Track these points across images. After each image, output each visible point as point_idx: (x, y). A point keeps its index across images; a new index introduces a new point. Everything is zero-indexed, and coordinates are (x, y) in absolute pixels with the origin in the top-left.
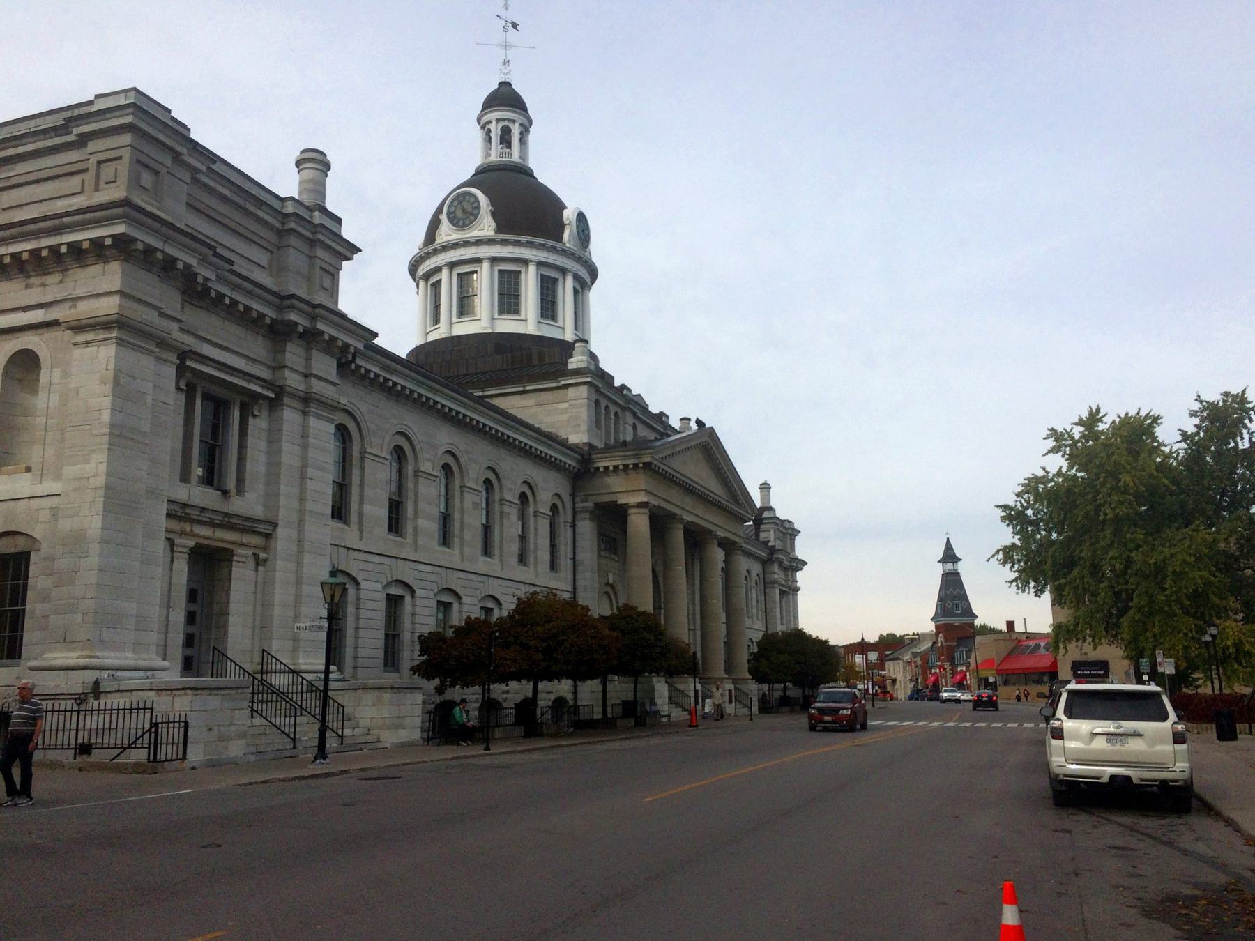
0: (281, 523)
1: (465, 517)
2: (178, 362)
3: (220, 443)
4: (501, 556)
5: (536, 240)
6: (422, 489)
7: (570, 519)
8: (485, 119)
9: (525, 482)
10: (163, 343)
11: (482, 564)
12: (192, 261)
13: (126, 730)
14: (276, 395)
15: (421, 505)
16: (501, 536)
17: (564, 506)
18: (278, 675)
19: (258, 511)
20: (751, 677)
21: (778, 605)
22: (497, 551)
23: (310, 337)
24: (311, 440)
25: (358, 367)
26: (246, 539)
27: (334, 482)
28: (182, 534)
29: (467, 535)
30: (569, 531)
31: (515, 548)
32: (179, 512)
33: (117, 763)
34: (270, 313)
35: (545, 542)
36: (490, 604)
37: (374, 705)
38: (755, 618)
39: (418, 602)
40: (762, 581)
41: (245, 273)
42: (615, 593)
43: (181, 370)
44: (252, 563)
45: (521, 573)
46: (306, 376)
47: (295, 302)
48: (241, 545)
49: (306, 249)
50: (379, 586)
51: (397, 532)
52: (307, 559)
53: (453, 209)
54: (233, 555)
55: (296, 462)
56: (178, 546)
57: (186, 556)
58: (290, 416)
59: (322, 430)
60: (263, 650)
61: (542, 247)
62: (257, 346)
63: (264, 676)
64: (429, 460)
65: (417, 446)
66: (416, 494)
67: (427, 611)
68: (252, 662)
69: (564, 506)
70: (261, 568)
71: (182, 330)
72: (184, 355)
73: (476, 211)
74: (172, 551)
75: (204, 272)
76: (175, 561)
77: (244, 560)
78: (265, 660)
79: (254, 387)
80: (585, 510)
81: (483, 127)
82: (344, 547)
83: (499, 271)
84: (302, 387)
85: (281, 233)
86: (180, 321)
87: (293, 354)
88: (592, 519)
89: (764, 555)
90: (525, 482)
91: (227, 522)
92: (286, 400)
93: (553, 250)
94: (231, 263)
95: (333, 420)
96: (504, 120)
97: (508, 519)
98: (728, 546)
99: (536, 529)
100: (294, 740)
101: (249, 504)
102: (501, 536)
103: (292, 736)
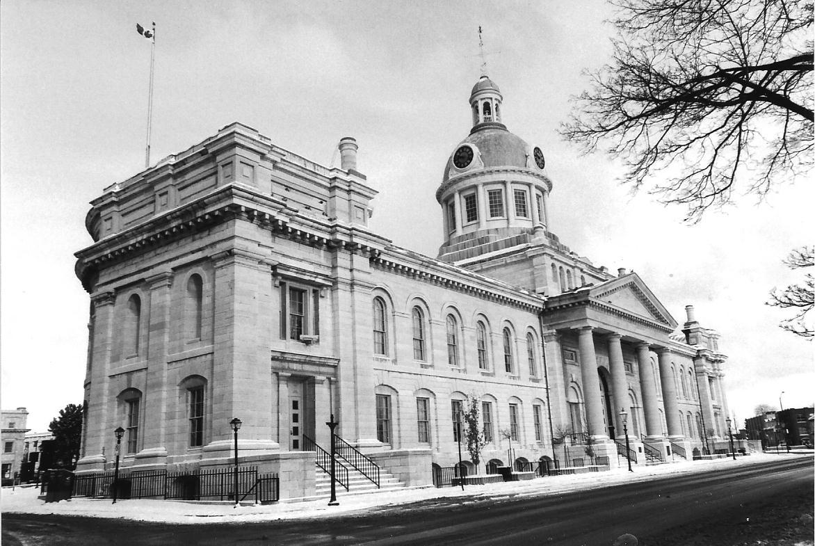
12: (274, 213)
15: (434, 341)
16: (493, 355)
19: (328, 353)
23: (351, 248)
26: (323, 369)
28: (283, 369)
34: (326, 237)
35: (524, 356)
43: (275, 275)
44: (327, 382)
48: (320, 373)
50: (411, 393)
58: (343, 294)
59: (364, 300)
62: (321, 256)
74: (278, 380)
75: (281, 218)
76: (280, 385)
79: (319, 280)
85: (332, 189)
87: (343, 258)
88: (557, 341)
91: (308, 361)
92: (340, 286)
98: (659, 350)
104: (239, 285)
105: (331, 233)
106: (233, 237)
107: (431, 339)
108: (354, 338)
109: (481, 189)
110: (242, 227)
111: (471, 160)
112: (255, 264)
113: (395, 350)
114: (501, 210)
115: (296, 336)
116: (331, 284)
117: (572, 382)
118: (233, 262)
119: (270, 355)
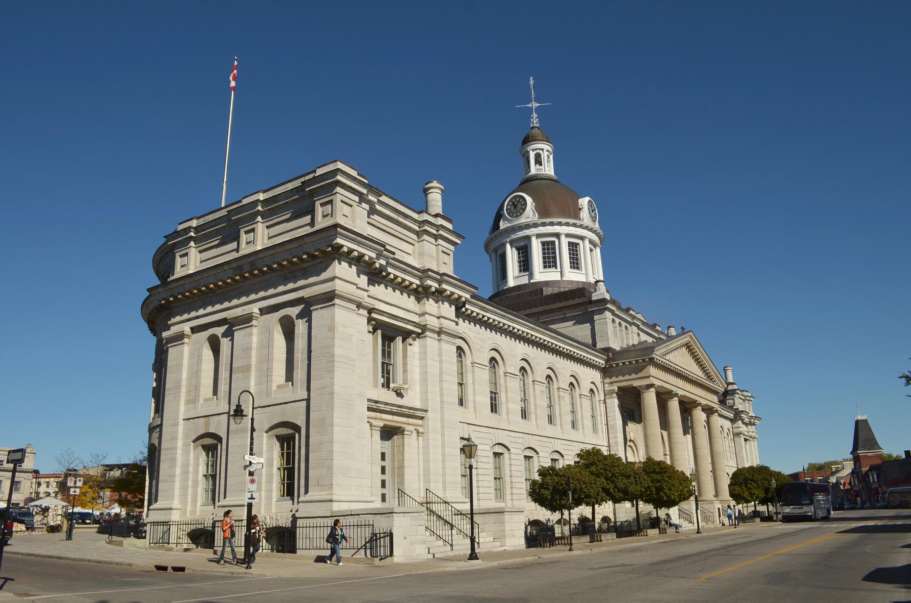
0: (429, 410)
1: (537, 400)
2: (368, 315)
3: (392, 363)
4: (561, 425)
5: (564, 220)
6: (509, 384)
7: (603, 398)
8: (523, 152)
9: (572, 376)
10: (359, 306)
11: (549, 430)
13: (359, 539)
14: (422, 330)
16: (560, 410)
17: (598, 390)
18: (439, 504)
19: (417, 404)
20: (732, 499)
21: (744, 449)
22: (558, 422)
24: (444, 357)
25: (467, 310)
26: (411, 421)
27: (458, 383)
29: (539, 412)
30: (603, 406)
31: (569, 418)
32: (374, 407)
33: (355, 558)
35: (588, 414)
36: (556, 456)
37: (495, 523)
38: (729, 459)
39: (513, 456)
40: (731, 432)
41: (401, 259)
42: (636, 446)
43: (370, 320)
44: (415, 433)
45: (574, 435)
46: (438, 318)
47: (430, 273)
49: (433, 240)
50: (488, 448)
51: (496, 412)
52: (446, 432)
53: (509, 207)
54: (404, 430)
55: (437, 372)
56: (374, 426)
57: (379, 432)
60: (427, 489)
61: (567, 224)
63: (428, 505)
64: (513, 365)
65: (504, 357)
66: (506, 387)
67: (518, 462)
68: (419, 497)
69: (598, 390)
70: (420, 439)
71: (369, 296)
72: (371, 311)
73: (523, 207)
77: (410, 433)
78: (428, 496)
80: (612, 392)
81: (524, 155)
82: (467, 423)
83: (541, 242)
84: (437, 325)
86: (367, 291)
87: (430, 305)
89: (731, 416)
90: (572, 376)
93: (574, 225)
94: (393, 253)
95: (455, 344)
96: (536, 149)
97: (564, 401)
99: (581, 406)
100: (452, 545)
101: (412, 399)
102: (560, 410)
103: (450, 543)
104: (339, 329)
105: (420, 279)
106: (333, 279)
107: (506, 392)
108: (441, 389)
109: (534, 239)
110: (342, 269)
111: (524, 210)
112: (354, 307)
113: (474, 402)
114: (555, 262)
115: (387, 385)
116: (420, 331)
117: (630, 441)
118: (334, 305)
119: (366, 404)
